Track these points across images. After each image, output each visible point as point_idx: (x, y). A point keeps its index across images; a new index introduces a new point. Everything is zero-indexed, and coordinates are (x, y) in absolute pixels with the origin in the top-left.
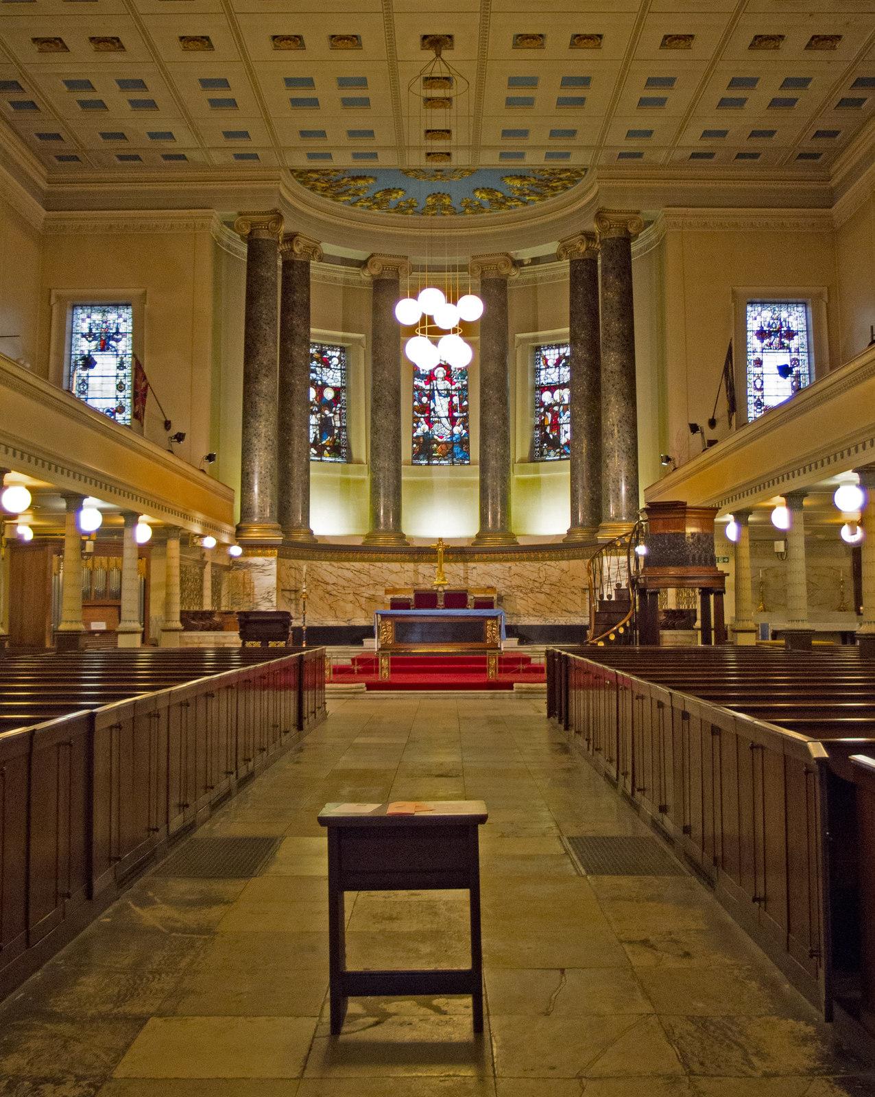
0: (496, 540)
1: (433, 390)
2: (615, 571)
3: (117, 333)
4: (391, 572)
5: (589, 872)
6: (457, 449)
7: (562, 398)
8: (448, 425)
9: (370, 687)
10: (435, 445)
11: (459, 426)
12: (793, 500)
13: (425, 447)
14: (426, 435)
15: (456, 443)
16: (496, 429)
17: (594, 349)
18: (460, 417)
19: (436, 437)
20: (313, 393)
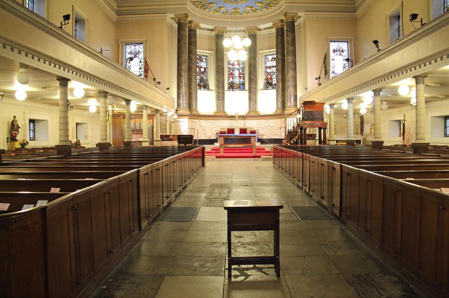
0: (253, 114)
2: (292, 123)
3: (139, 52)
4: (222, 123)
5: (302, 219)
6: (241, 86)
7: (273, 71)
9: (217, 157)
12: (349, 100)
13: (232, 86)
14: (232, 82)
16: (253, 80)
17: (283, 55)
20: (198, 69)
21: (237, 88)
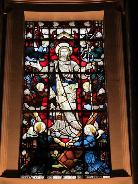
1: (54, 73)
6: (90, 158)
8: (75, 124)
10: (56, 152)
11: (92, 123)
14: (41, 136)
15: (90, 149)
18: (95, 111)
19: (57, 140)
21: (69, 169)
